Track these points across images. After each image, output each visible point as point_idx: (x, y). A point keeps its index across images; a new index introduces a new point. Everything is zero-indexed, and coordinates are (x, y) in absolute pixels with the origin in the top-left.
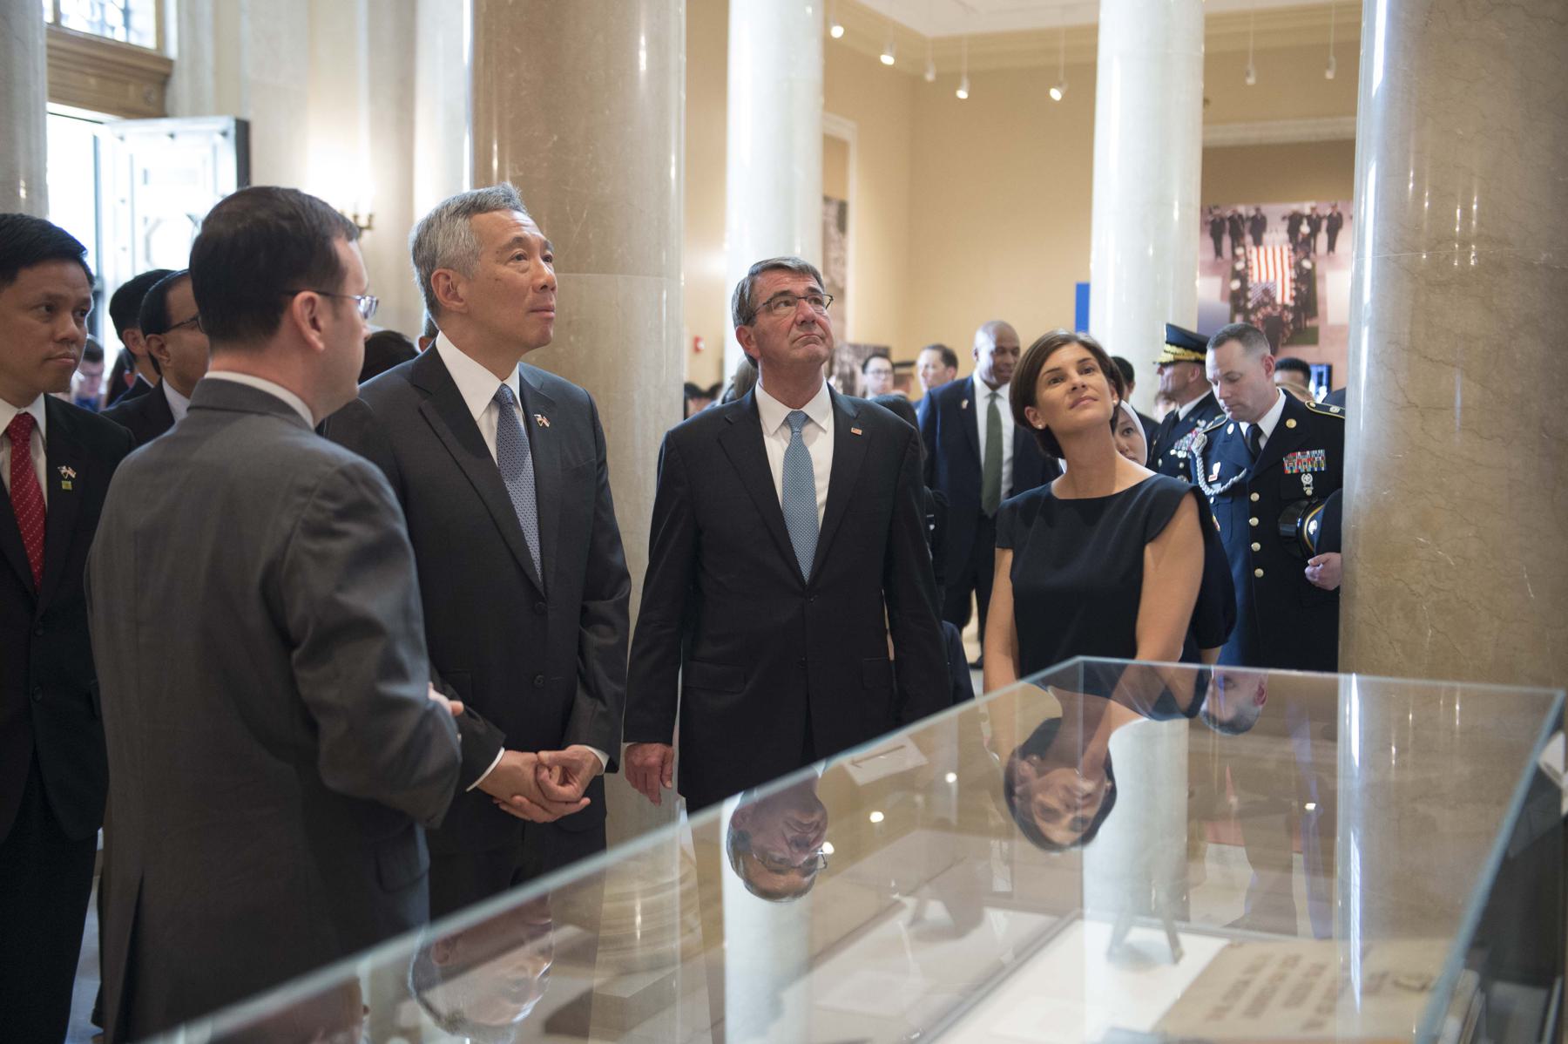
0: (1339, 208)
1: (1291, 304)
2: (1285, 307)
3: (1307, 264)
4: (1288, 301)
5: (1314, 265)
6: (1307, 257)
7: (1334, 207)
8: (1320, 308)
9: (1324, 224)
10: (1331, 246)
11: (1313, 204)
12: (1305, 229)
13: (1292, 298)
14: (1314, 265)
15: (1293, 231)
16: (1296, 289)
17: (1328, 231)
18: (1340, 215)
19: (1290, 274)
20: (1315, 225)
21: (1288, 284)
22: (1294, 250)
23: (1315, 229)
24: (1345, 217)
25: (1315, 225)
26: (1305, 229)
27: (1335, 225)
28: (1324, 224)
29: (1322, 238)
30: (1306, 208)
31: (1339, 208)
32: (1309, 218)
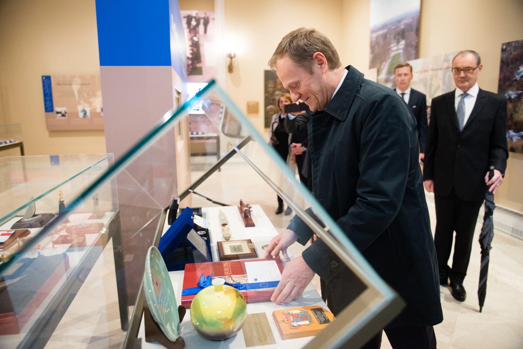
0: (208, 15)
1: (190, 56)
2: (188, 58)
3: (195, 39)
5: (199, 39)
6: (195, 36)
7: (205, 13)
8: (202, 59)
9: (202, 21)
10: (205, 31)
12: (194, 23)
13: (192, 54)
14: (199, 39)
16: (192, 50)
19: (189, 43)
20: (198, 21)
22: (190, 32)
24: (210, 19)
25: (198, 21)
28: (202, 21)
30: (193, 13)
32: (195, 17)
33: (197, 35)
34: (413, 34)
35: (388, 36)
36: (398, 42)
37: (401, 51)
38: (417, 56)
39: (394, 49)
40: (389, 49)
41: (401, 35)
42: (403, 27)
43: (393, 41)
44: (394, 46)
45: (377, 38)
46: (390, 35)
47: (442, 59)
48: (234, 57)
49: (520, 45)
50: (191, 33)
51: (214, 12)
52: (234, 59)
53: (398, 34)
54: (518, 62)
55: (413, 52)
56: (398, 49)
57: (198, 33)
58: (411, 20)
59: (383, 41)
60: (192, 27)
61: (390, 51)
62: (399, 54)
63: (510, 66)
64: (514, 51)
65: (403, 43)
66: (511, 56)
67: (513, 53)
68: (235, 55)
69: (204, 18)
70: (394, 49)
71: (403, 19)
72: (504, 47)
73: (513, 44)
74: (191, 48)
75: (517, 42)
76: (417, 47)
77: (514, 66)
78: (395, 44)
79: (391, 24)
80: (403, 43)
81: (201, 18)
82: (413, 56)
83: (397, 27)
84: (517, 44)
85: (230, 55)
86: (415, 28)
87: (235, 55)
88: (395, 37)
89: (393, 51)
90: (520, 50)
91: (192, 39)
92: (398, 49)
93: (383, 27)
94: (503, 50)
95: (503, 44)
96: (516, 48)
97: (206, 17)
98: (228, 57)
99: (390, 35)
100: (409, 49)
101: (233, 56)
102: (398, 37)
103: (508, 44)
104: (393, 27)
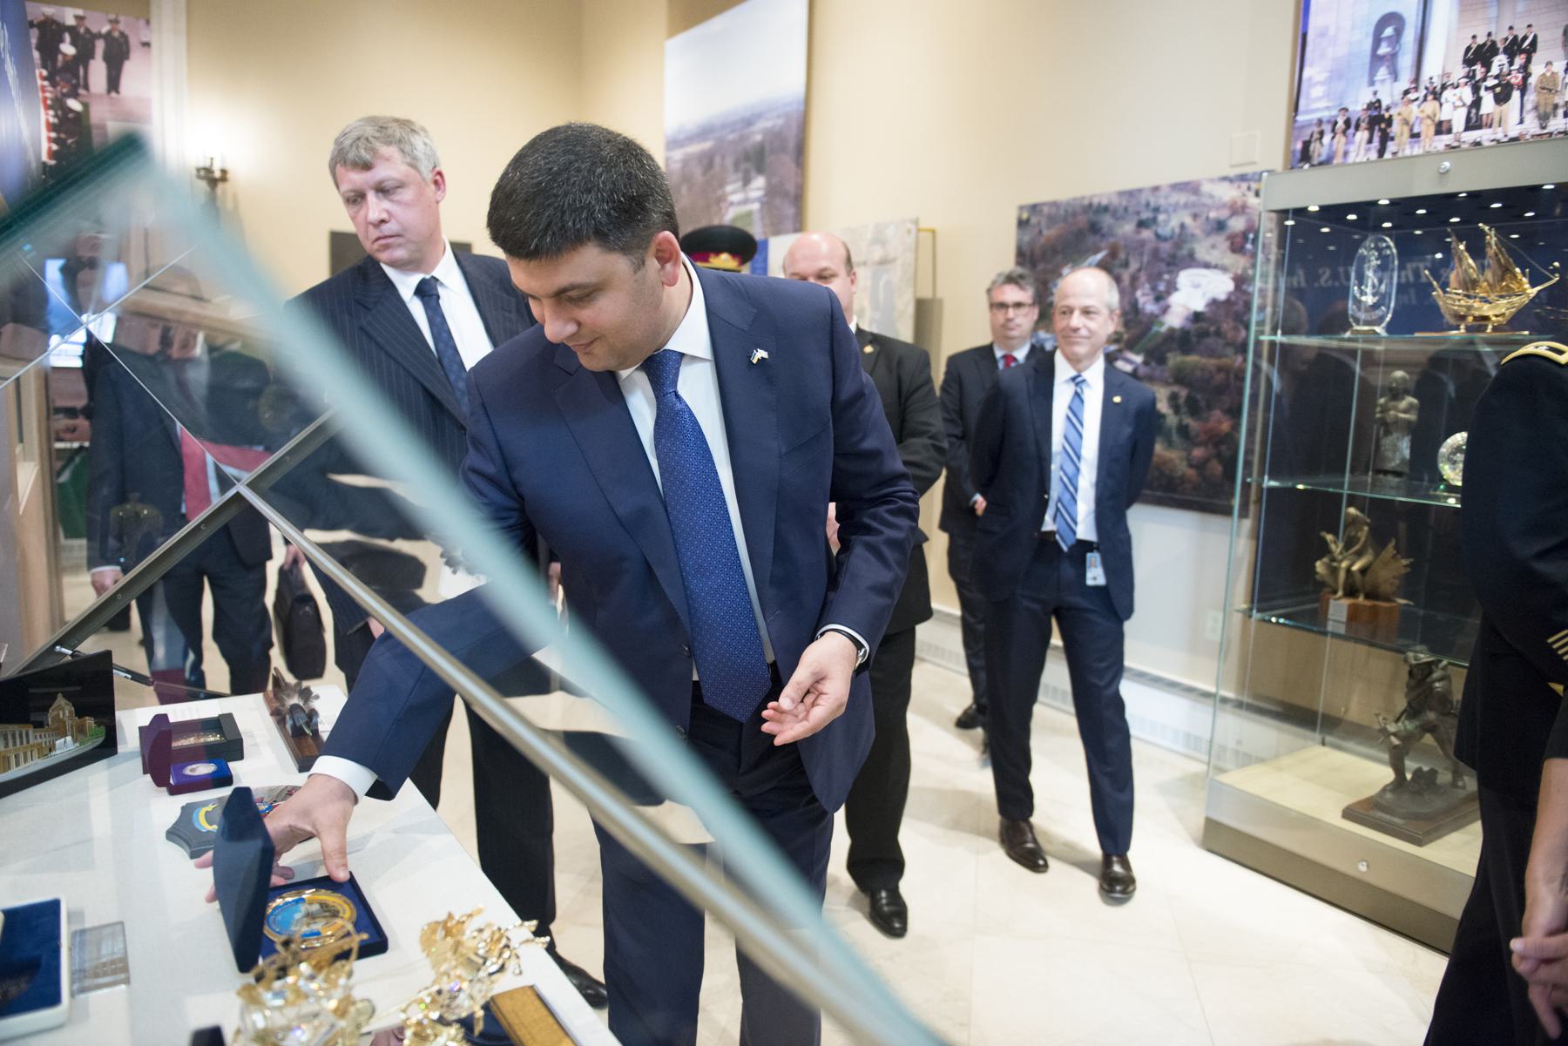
0: (121, 27)
1: (53, 162)
3: (74, 104)
4: (45, 158)
5: (86, 106)
6: (75, 96)
9: (100, 46)
10: (114, 84)
11: (80, 12)
12: (68, 49)
13: (52, 154)
14: (86, 106)
15: (49, 48)
16: (55, 141)
17: (106, 58)
18: (122, 34)
20: (85, 44)
21: (44, 134)
22: (50, 78)
23: (85, 55)
24: (133, 41)
26: (68, 49)
27: (117, 56)
28: (100, 46)
29: (98, 71)
30: (69, 16)
31: (121, 27)
32: (72, 30)
33: (81, 91)
34: (788, 161)
35: (717, 160)
36: (746, 181)
37: (756, 206)
38: (799, 225)
39: (735, 198)
40: (721, 199)
41: (755, 159)
42: (758, 138)
43: (733, 177)
44: (734, 192)
45: (686, 162)
46: (723, 157)
47: (869, 236)
48: (224, 177)
49: (1062, 212)
50: (54, 84)
51: (148, 22)
52: (220, 186)
53: (747, 157)
54: (1059, 258)
55: (790, 211)
56: (746, 201)
57: (86, 87)
58: (780, 122)
59: (705, 173)
60: (60, 58)
61: (723, 205)
62: (749, 214)
63: (1041, 266)
64: (1048, 228)
65: (759, 182)
66: (1042, 240)
67: (1046, 232)
68: (224, 172)
69: (108, 37)
70: (735, 198)
71: (759, 116)
72: (1025, 216)
73: (1046, 210)
74: (53, 135)
75: (1055, 204)
76: (798, 199)
77: (1049, 266)
78: (739, 184)
79: (724, 126)
80: (759, 182)
81: (99, 36)
82: (789, 224)
83: (742, 138)
84: (1054, 210)
85: (209, 171)
86: (791, 144)
87: (224, 172)
88: (736, 165)
89: (732, 204)
90: (1061, 225)
91: (58, 105)
92: (746, 201)
93: (704, 133)
94: (1022, 224)
95: (1021, 208)
96: (1052, 220)
97: (116, 34)
98: (199, 177)
99: (723, 157)
100: (778, 201)
101: (217, 174)
102: (748, 165)
103: (1034, 208)
104: (731, 137)
